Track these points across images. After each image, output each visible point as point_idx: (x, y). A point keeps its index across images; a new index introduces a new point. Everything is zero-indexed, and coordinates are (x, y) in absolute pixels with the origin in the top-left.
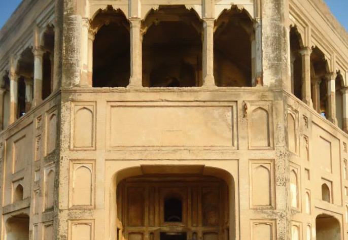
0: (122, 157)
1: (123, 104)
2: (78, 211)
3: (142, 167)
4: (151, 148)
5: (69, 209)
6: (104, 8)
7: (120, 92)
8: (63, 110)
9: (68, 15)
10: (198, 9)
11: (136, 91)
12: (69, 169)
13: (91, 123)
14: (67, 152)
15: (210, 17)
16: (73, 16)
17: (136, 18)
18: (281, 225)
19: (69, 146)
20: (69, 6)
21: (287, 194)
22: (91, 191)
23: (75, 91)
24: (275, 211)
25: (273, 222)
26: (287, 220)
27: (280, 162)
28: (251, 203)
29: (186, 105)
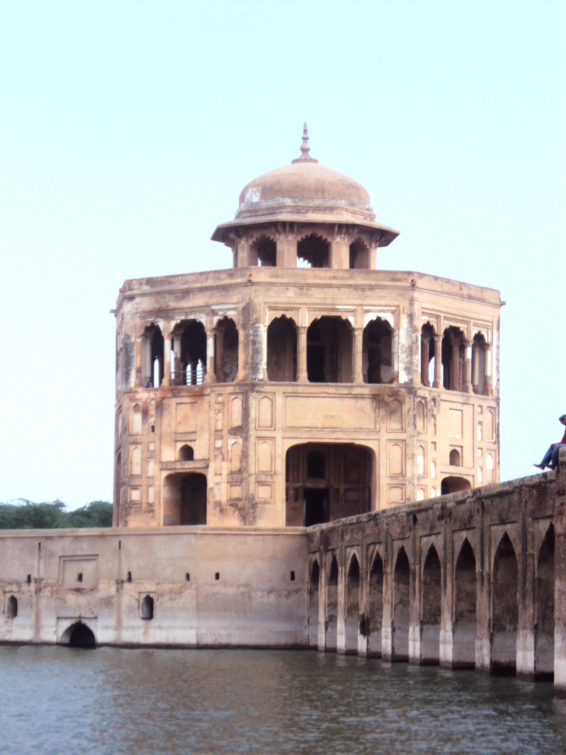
0: (294, 435)
1: (295, 395)
4: (315, 429)
5: (256, 474)
6: (279, 316)
8: (251, 398)
9: (254, 324)
10: (351, 319)
12: (255, 444)
13: (270, 409)
15: (360, 327)
16: (257, 325)
17: (305, 327)
18: (409, 488)
19: (255, 427)
20: (254, 317)
22: (272, 461)
23: (260, 385)
24: (405, 478)
25: (404, 486)
26: (413, 484)
27: (409, 441)
28: (388, 472)
29: (342, 396)
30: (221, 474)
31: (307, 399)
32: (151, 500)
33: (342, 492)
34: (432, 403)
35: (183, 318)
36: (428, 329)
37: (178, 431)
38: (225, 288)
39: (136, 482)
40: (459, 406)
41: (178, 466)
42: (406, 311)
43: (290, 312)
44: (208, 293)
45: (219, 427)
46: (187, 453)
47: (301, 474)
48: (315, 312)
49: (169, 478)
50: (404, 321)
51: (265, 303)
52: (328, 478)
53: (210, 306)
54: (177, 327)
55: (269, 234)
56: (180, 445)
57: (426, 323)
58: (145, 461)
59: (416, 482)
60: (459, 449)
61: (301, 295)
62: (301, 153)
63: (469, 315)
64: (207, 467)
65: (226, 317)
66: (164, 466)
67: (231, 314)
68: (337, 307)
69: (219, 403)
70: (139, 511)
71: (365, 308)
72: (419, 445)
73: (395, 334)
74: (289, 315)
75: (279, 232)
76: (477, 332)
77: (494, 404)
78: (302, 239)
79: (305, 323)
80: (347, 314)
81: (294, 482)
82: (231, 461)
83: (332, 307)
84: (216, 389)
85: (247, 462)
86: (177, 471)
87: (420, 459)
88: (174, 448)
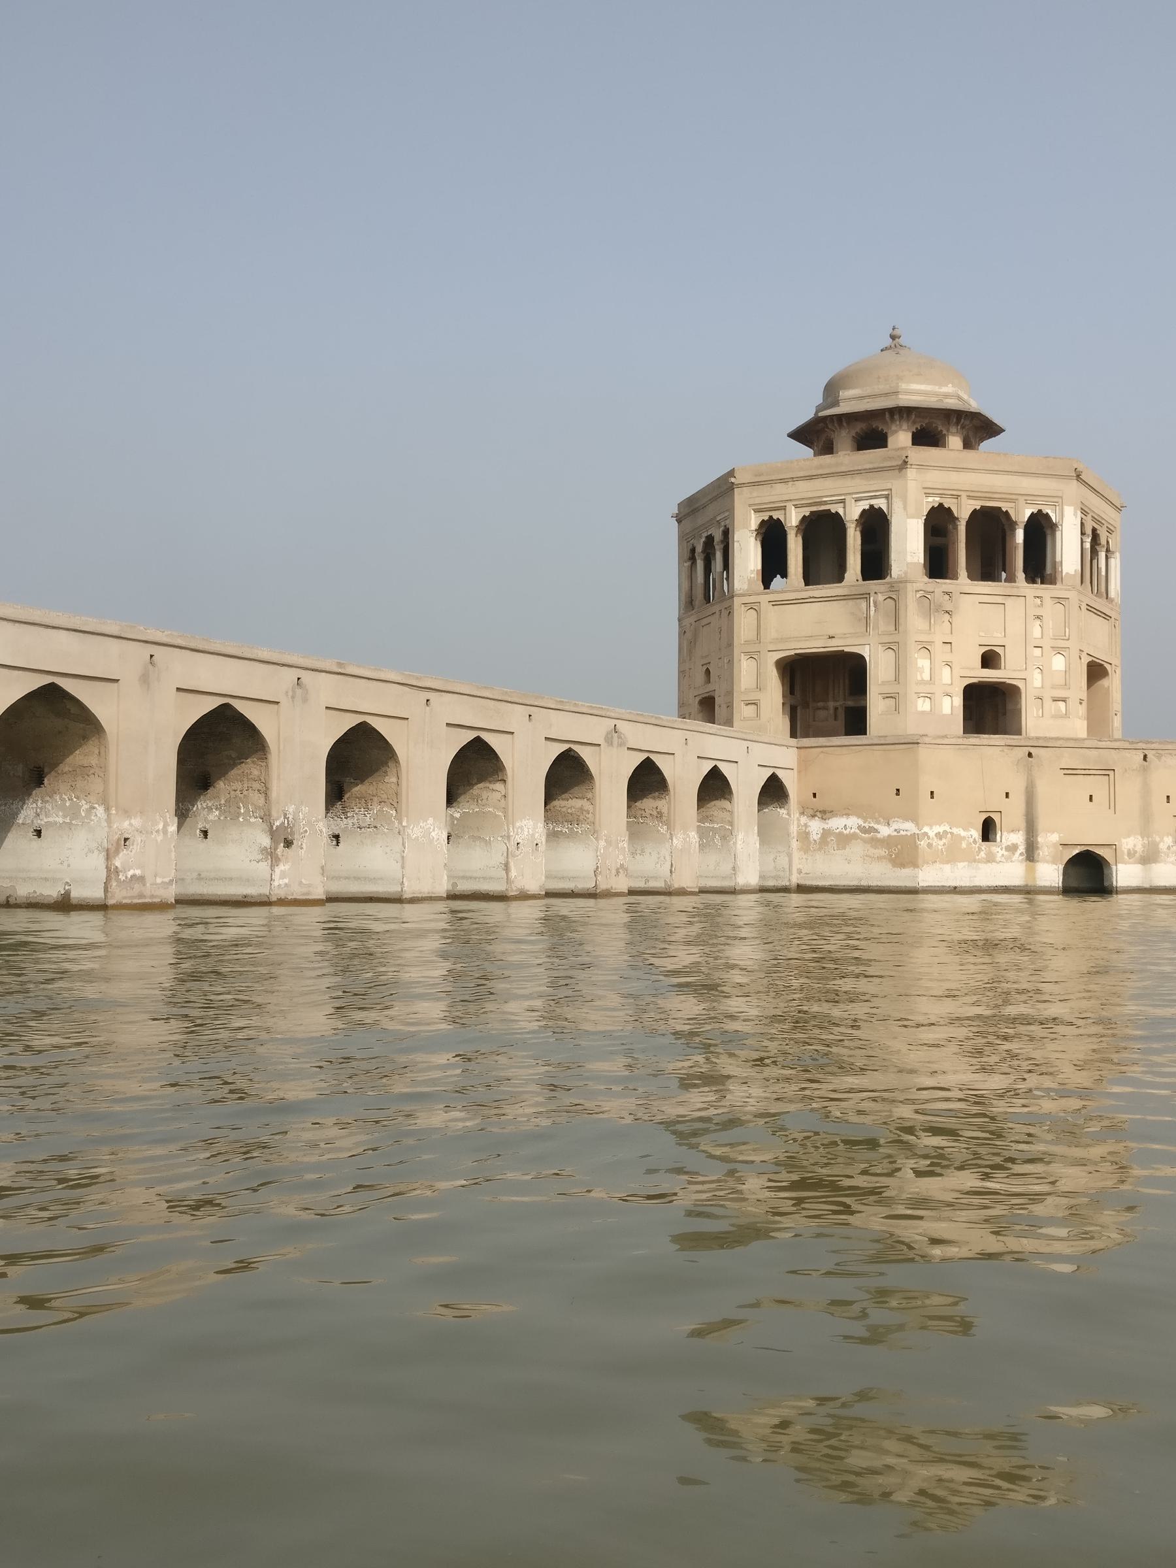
6: (766, 518)
10: (841, 512)
60: (999, 650)
74: (776, 515)
87: (923, 663)
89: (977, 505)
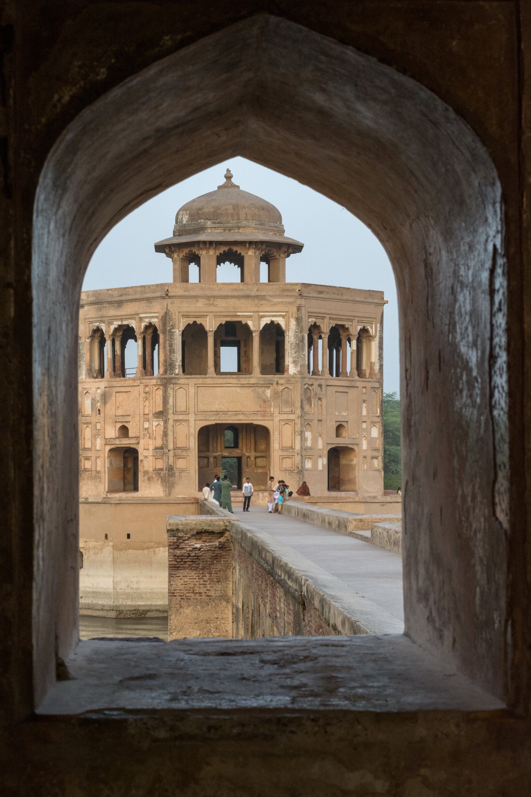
0: (204, 418)
2: (180, 451)
3: (217, 424)
4: (221, 413)
6: (191, 323)
7: (203, 378)
10: (250, 323)
11: (213, 378)
13: (185, 397)
14: (172, 415)
20: (171, 324)
21: (303, 439)
29: (243, 386)
30: (148, 449)
31: (214, 388)
32: (99, 469)
33: (253, 459)
34: (319, 388)
35: (120, 323)
36: (314, 329)
37: (117, 415)
38: (149, 300)
39: (89, 454)
40: (346, 390)
41: (117, 442)
42: (293, 317)
43: (199, 319)
44: (138, 303)
45: (147, 412)
46: (124, 431)
47: (219, 445)
48: (220, 318)
49: (111, 450)
50: (293, 323)
51: (179, 312)
52: (230, 451)
53: (138, 314)
54: (116, 330)
55: (195, 250)
56: (119, 425)
57: (313, 324)
58: (94, 437)
59: (304, 453)
61: (209, 305)
62: (225, 180)
63: (353, 314)
64: (138, 443)
65: (150, 323)
66: (107, 442)
67: (155, 321)
68: (238, 314)
69: (146, 393)
70: (91, 478)
71: (260, 314)
72: (307, 423)
73: (286, 334)
74: (199, 321)
75: (202, 249)
76: (362, 327)
77: (377, 385)
78: (220, 254)
79: (212, 328)
80: (246, 319)
81: (214, 452)
82: (155, 439)
83: (234, 314)
84: (142, 381)
85: (167, 441)
86: (117, 446)
87: (308, 435)
88: (114, 428)
89: (333, 323)
